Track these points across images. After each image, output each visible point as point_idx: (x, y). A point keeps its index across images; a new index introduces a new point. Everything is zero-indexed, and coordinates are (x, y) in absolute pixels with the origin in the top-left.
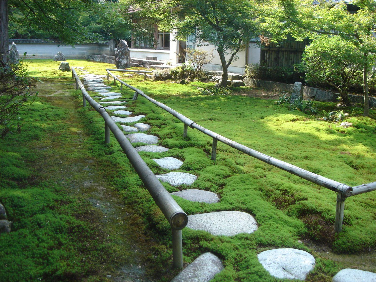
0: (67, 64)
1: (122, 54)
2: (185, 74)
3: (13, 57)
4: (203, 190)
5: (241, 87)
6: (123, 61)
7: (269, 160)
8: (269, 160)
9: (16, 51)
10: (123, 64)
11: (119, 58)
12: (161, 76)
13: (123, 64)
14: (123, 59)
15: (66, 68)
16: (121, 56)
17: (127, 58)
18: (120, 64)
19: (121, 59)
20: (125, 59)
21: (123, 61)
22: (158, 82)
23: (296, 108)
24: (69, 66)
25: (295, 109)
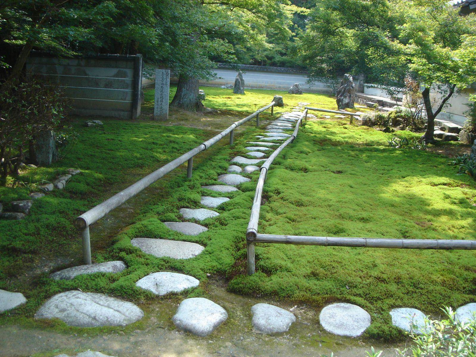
0: (280, 99)
1: (344, 91)
2: (399, 121)
3: (237, 86)
4: (203, 225)
5: (452, 142)
6: (344, 99)
7: (366, 243)
8: (366, 243)
9: (242, 80)
10: (344, 103)
11: (341, 96)
12: (370, 120)
13: (344, 103)
14: (345, 97)
15: (278, 103)
16: (343, 93)
17: (350, 97)
18: (340, 103)
19: (342, 97)
20: (347, 97)
21: (344, 99)
22: (365, 127)
23: (466, 172)
24: (282, 101)
25: (464, 173)
